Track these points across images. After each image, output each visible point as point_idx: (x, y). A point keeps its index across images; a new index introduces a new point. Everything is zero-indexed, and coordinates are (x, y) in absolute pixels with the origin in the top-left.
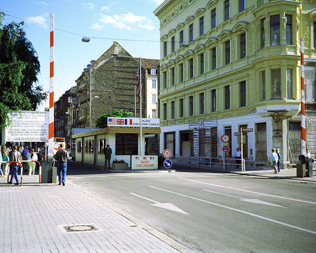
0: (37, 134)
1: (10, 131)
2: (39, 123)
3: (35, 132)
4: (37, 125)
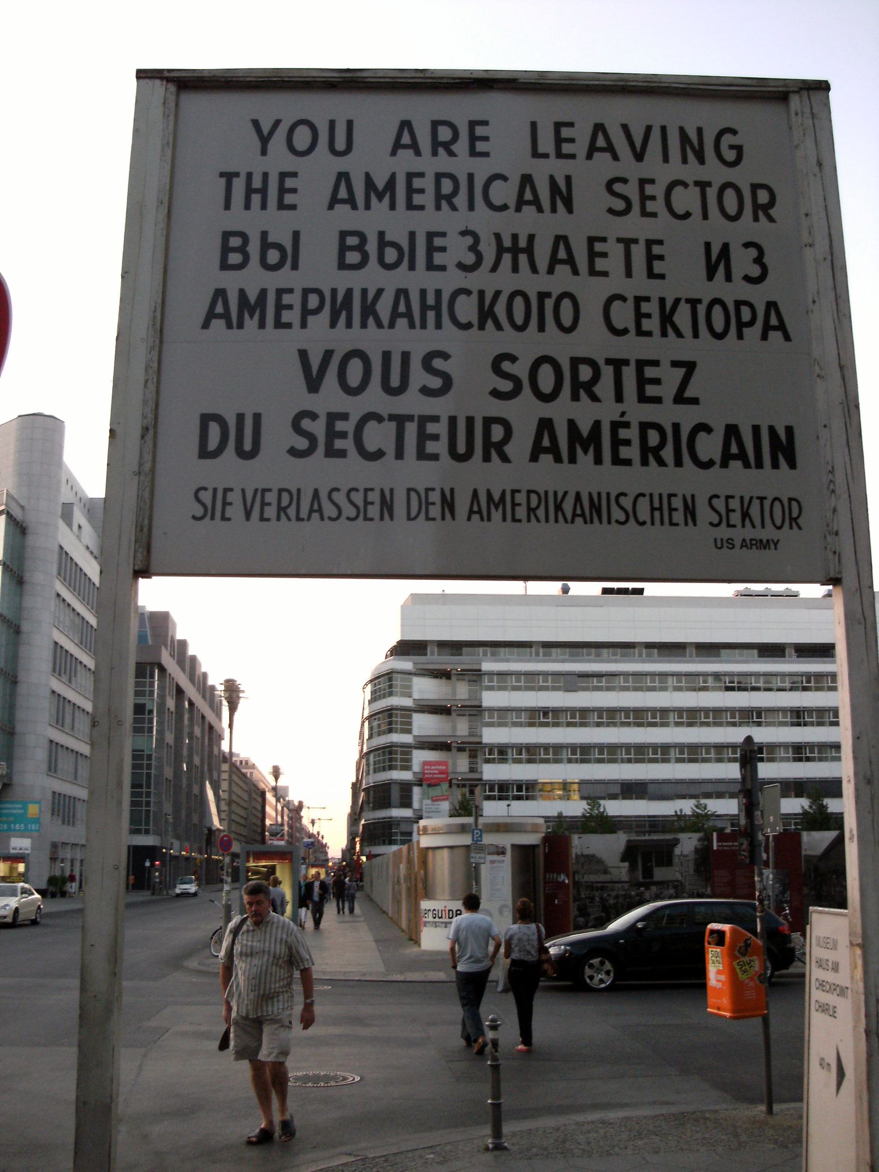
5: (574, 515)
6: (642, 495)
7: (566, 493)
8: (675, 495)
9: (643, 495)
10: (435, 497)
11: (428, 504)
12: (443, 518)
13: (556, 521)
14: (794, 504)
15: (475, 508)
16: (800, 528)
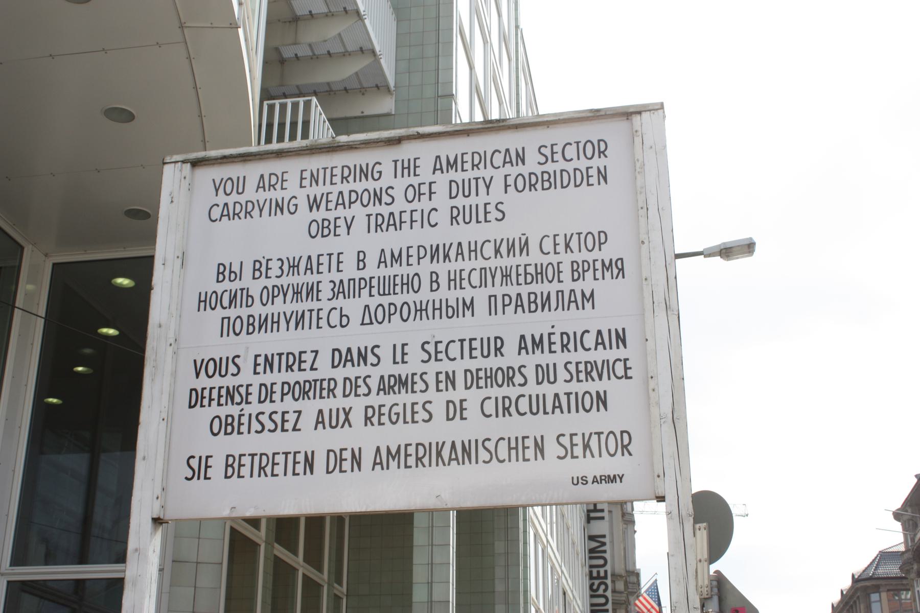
1: (204, 382)
2: (535, 257)
3: (491, 377)
4: (513, 290)
5: (450, 459)
7: (444, 443)
8: (528, 437)
9: (503, 439)
10: (347, 455)
11: (342, 460)
12: (352, 471)
13: (437, 465)
14: (625, 435)
15: (378, 461)
16: (630, 454)
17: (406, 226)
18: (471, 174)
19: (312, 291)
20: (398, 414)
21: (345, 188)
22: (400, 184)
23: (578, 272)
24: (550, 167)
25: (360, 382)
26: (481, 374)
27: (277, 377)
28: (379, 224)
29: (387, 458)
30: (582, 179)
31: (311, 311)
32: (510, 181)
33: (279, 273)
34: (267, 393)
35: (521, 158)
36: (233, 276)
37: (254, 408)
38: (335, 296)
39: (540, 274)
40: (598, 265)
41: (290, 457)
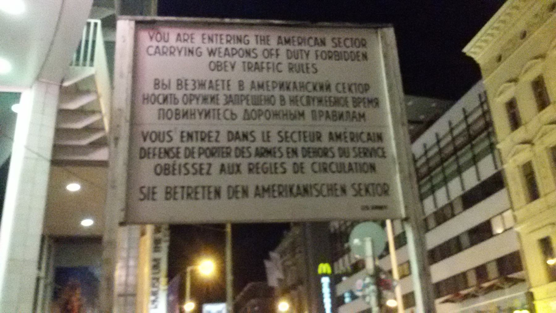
0: (328, 160)
2: (333, 93)
3: (316, 152)
4: (324, 109)
6: (324, 184)
10: (240, 189)
17: (265, 71)
18: (298, 48)
19: (214, 99)
20: (267, 168)
21: (229, 46)
22: (260, 48)
23: (357, 102)
24: (338, 49)
25: (245, 150)
26: (311, 150)
27: (196, 144)
28: (250, 67)
29: (263, 191)
30: (355, 57)
31: (214, 110)
32: (319, 53)
33: (193, 87)
34: (190, 153)
35: (323, 43)
36: (164, 87)
37: (182, 161)
38: (227, 103)
39: (337, 102)
40: (366, 101)
41: (206, 189)
